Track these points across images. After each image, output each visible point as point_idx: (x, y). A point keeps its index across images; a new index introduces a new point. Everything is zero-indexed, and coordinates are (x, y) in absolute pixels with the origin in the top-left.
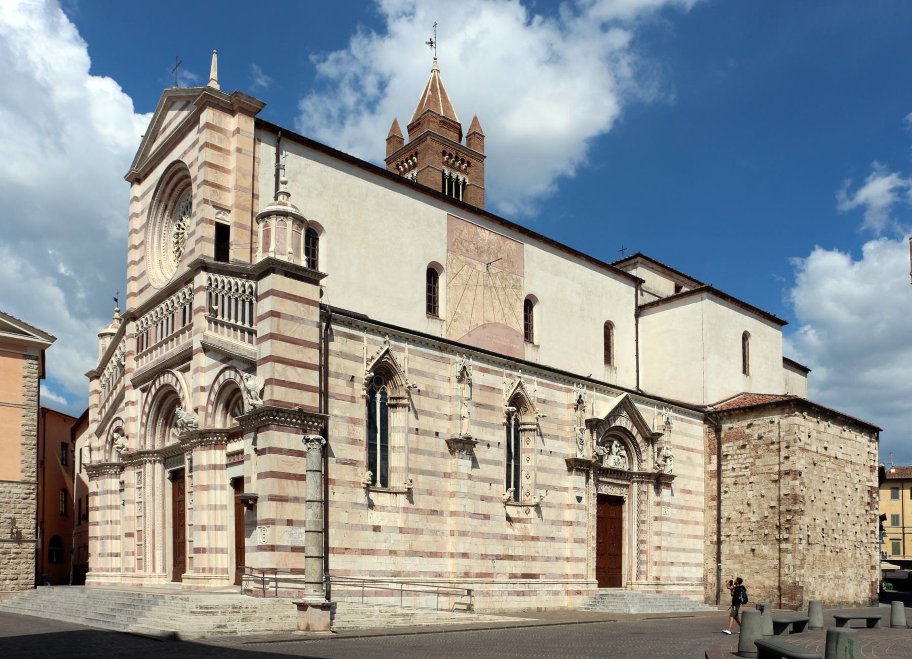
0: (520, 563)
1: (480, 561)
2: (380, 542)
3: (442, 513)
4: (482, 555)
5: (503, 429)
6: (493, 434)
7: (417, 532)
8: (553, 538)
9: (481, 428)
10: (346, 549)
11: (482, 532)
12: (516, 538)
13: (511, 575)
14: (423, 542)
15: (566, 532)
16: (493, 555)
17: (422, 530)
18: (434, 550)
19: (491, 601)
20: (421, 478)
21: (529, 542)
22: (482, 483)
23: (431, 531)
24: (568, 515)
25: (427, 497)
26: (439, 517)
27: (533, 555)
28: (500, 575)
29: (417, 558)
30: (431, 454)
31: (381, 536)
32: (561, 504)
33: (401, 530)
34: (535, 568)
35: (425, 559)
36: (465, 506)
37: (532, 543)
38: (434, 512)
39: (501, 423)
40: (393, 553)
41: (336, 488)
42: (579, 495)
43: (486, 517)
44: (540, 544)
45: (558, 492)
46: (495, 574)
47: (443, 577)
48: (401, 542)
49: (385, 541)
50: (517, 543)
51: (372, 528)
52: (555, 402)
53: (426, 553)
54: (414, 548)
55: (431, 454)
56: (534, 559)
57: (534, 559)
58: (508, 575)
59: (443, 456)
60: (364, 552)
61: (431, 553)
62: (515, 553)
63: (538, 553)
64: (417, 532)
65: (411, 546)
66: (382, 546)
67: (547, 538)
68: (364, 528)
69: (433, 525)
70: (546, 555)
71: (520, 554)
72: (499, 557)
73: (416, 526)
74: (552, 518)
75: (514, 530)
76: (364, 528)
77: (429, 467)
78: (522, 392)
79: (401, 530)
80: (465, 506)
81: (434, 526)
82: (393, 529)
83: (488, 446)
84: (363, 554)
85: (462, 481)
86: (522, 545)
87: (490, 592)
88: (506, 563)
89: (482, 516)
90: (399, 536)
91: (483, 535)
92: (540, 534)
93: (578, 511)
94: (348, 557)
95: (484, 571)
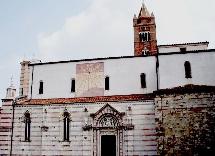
6: (56, 124)
7: (34, 150)
33: (29, 150)
37: (70, 152)
41: (14, 142)
42: (86, 137)
43: (53, 146)
64: (34, 150)
65: (31, 154)
68: (20, 150)
76: (20, 150)
78: (67, 111)
79: (29, 150)
82: (27, 150)
83: (54, 127)
91: (52, 150)
92: (72, 149)
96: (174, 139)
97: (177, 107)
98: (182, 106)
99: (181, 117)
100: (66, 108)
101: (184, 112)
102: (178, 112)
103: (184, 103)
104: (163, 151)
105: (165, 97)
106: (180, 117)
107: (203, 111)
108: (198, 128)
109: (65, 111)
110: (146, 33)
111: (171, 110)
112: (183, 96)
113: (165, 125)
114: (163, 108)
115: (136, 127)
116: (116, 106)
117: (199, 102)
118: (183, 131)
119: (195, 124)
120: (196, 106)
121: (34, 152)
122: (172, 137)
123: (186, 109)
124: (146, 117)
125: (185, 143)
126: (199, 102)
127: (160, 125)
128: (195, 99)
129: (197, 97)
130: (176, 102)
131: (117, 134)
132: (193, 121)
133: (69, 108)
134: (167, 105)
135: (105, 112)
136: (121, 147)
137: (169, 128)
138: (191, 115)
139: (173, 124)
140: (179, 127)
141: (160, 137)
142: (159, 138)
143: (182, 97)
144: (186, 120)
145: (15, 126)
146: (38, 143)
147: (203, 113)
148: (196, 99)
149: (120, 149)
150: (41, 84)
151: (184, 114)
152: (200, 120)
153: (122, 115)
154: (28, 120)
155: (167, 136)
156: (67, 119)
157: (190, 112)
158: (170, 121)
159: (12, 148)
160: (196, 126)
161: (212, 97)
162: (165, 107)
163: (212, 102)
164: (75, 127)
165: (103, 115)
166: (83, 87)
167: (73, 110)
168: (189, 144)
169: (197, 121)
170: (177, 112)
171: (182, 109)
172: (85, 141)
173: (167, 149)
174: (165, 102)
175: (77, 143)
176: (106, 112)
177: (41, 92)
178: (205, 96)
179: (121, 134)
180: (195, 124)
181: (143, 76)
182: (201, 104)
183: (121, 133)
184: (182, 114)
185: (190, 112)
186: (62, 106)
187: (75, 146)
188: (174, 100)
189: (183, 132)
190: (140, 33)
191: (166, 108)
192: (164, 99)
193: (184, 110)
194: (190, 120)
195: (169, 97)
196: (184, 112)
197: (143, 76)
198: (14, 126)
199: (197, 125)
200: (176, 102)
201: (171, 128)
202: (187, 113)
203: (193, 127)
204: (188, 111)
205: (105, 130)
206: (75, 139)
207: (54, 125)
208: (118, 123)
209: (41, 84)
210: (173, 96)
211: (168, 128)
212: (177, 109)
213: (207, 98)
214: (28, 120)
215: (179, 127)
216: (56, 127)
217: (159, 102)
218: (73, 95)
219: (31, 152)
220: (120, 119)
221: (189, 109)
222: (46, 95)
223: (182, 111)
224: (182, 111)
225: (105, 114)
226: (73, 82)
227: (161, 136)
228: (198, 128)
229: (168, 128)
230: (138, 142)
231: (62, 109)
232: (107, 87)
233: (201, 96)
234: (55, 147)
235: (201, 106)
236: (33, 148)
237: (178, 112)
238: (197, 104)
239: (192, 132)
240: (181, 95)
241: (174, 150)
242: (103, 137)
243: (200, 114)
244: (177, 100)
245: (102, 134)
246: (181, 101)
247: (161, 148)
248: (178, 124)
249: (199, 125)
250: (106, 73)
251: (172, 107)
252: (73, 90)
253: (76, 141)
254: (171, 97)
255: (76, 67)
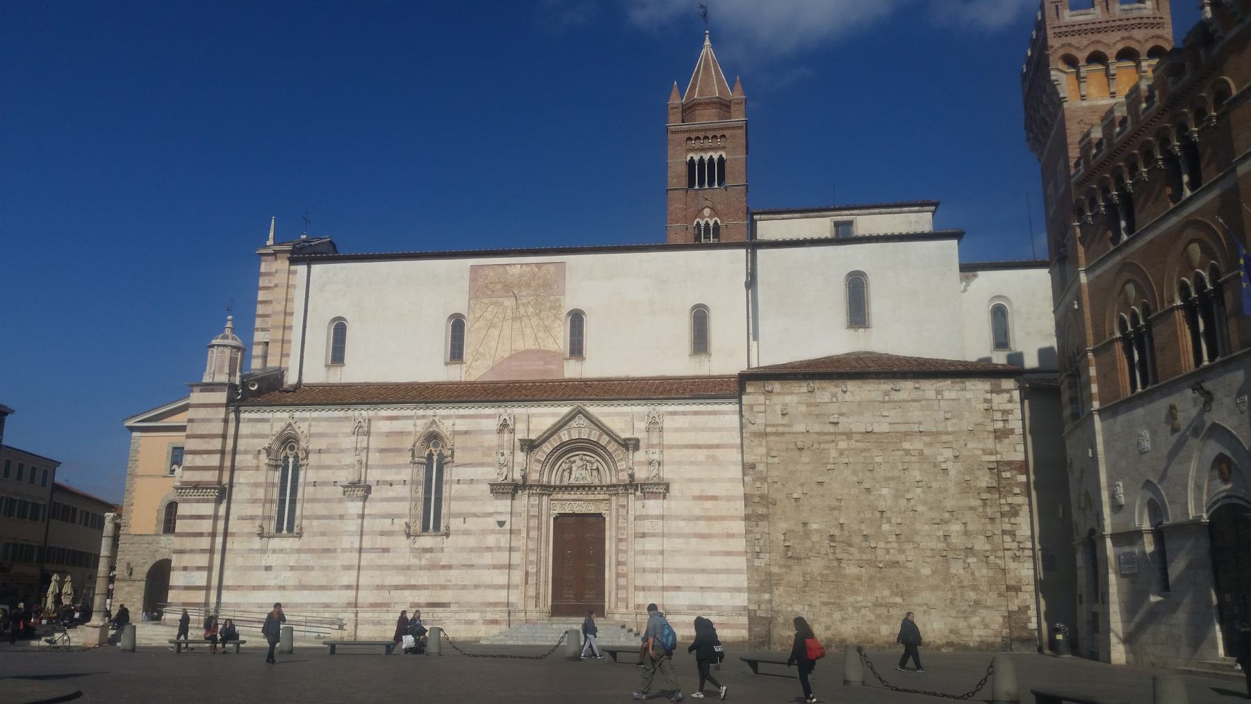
0: (426, 593)
1: (374, 592)
2: (270, 579)
3: (335, 551)
4: (378, 586)
5: (410, 468)
7: (309, 568)
8: (471, 566)
9: (385, 471)
10: (239, 586)
11: (380, 564)
12: (421, 568)
13: (413, 605)
14: (314, 577)
15: (488, 558)
16: (391, 586)
17: (313, 567)
18: (324, 582)
19: (383, 629)
20: (315, 523)
21: (438, 571)
22: (382, 520)
23: (322, 567)
24: (491, 541)
25: (321, 538)
26: (331, 555)
27: (442, 584)
28: (399, 604)
29: (305, 592)
30: (327, 501)
31: (272, 574)
32: (483, 530)
33: (292, 568)
34: (444, 597)
35: (313, 592)
36: (352, 543)
37: (442, 572)
38: (327, 550)
39: (409, 462)
40: (282, 588)
42: (501, 519)
43: (386, 550)
44: (452, 572)
45: (481, 519)
46: (392, 604)
47: (332, 607)
48: (289, 578)
49: (275, 578)
50: (422, 572)
51: (264, 568)
52: (481, 430)
53: (316, 586)
54: (303, 583)
55: (327, 501)
56: (444, 587)
57: (444, 587)
58: (409, 604)
59: (340, 500)
60: (254, 588)
61: (320, 586)
62: (420, 583)
63: (450, 581)
64: (309, 568)
65: (300, 581)
66: (272, 583)
67: (463, 565)
68: (257, 568)
69: (325, 561)
70: (461, 583)
71: (426, 583)
72: (397, 588)
73: (307, 563)
74: (469, 545)
75: (420, 560)
76: (257, 568)
77: (325, 513)
79: (292, 568)
80: (352, 543)
81: (325, 562)
83: (391, 485)
84: (253, 590)
85: (351, 521)
86: (428, 574)
87: (382, 622)
88: (407, 593)
89: (380, 550)
90: (289, 574)
91: (380, 568)
92: (454, 562)
93: (499, 536)
94: (240, 593)
95: (379, 601)
96: (807, 535)
97: (816, 428)
98: (836, 424)
99: (831, 461)
100: (436, 419)
101: (843, 445)
102: (819, 443)
103: (842, 414)
104: (769, 574)
105: (778, 394)
106: (826, 461)
107: (906, 445)
108: (889, 502)
109: (431, 430)
110: (711, 159)
111: (796, 435)
112: (839, 390)
113: (776, 486)
114: (769, 430)
115: (674, 489)
116: (609, 415)
117: (894, 415)
118: (839, 508)
119: (878, 486)
120: (884, 427)
121: (313, 574)
122: (800, 528)
123: (849, 435)
124: (708, 457)
125: (844, 551)
126: (892, 413)
127: (758, 484)
128: (880, 402)
129: (887, 398)
130: (816, 410)
131: (610, 510)
132: (874, 479)
133: (444, 417)
134: (786, 420)
135: (570, 435)
136: (622, 558)
137: (789, 496)
138: (865, 458)
139: (802, 485)
140: (823, 496)
141: (757, 526)
142: (755, 529)
143: (834, 395)
144: (847, 472)
145: (242, 480)
146: (323, 542)
147: (907, 452)
148: (884, 402)
149: (619, 563)
150: (339, 330)
151: (841, 453)
152: (896, 473)
153: (630, 445)
154: (291, 460)
155: (783, 526)
156: (435, 458)
157: (860, 445)
158: (792, 473)
159: (227, 564)
160: (880, 495)
161: (939, 397)
162: (777, 425)
163: (941, 415)
164: (464, 483)
165: (563, 444)
166: (494, 344)
167: (461, 425)
168: (857, 556)
169: (887, 479)
170: (816, 446)
171: (835, 434)
172: (499, 533)
173: (780, 567)
174: (778, 408)
175: (471, 542)
176: (575, 436)
177: (338, 356)
178: (915, 394)
179: (622, 512)
180: (878, 486)
181: (700, 318)
182: (899, 420)
183: (623, 506)
184: (833, 453)
185: (860, 445)
186: (421, 412)
187: (462, 549)
188: (809, 405)
189: (836, 512)
190: (689, 158)
191: (781, 429)
192: (776, 399)
193: (840, 437)
194: (860, 474)
195: (791, 393)
196: (843, 445)
197: (700, 318)
198: (235, 481)
199: (885, 491)
200: (816, 410)
201: (795, 496)
202: (854, 449)
203: (872, 497)
204: (856, 441)
205: (567, 497)
206: (462, 527)
207: (389, 478)
208: (613, 472)
209: (339, 330)
210: (804, 389)
211: (787, 497)
212: (819, 433)
213: (923, 402)
214: (291, 460)
215: (823, 496)
216: (398, 483)
217: (755, 409)
218: (456, 374)
219: (298, 573)
220: (621, 460)
221: (858, 437)
222: (354, 372)
223: (833, 441)
224: (833, 441)
225: (571, 441)
226: (458, 326)
227: (761, 523)
228: (889, 502)
229: (787, 497)
230: (681, 541)
231: (420, 422)
232: (577, 350)
233: (902, 395)
234: (391, 554)
235: (903, 428)
236: (306, 559)
237: (819, 443)
238: (888, 420)
239: (868, 515)
240: (834, 390)
241: (804, 574)
242: (562, 521)
243: (898, 453)
244: (817, 405)
245: (558, 510)
246: (834, 408)
247: (763, 564)
248: (821, 483)
249: (892, 491)
250: (569, 304)
251: (800, 427)
252: (456, 354)
253: (466, 533)
254: (797, 394)
255: (467, 275)
